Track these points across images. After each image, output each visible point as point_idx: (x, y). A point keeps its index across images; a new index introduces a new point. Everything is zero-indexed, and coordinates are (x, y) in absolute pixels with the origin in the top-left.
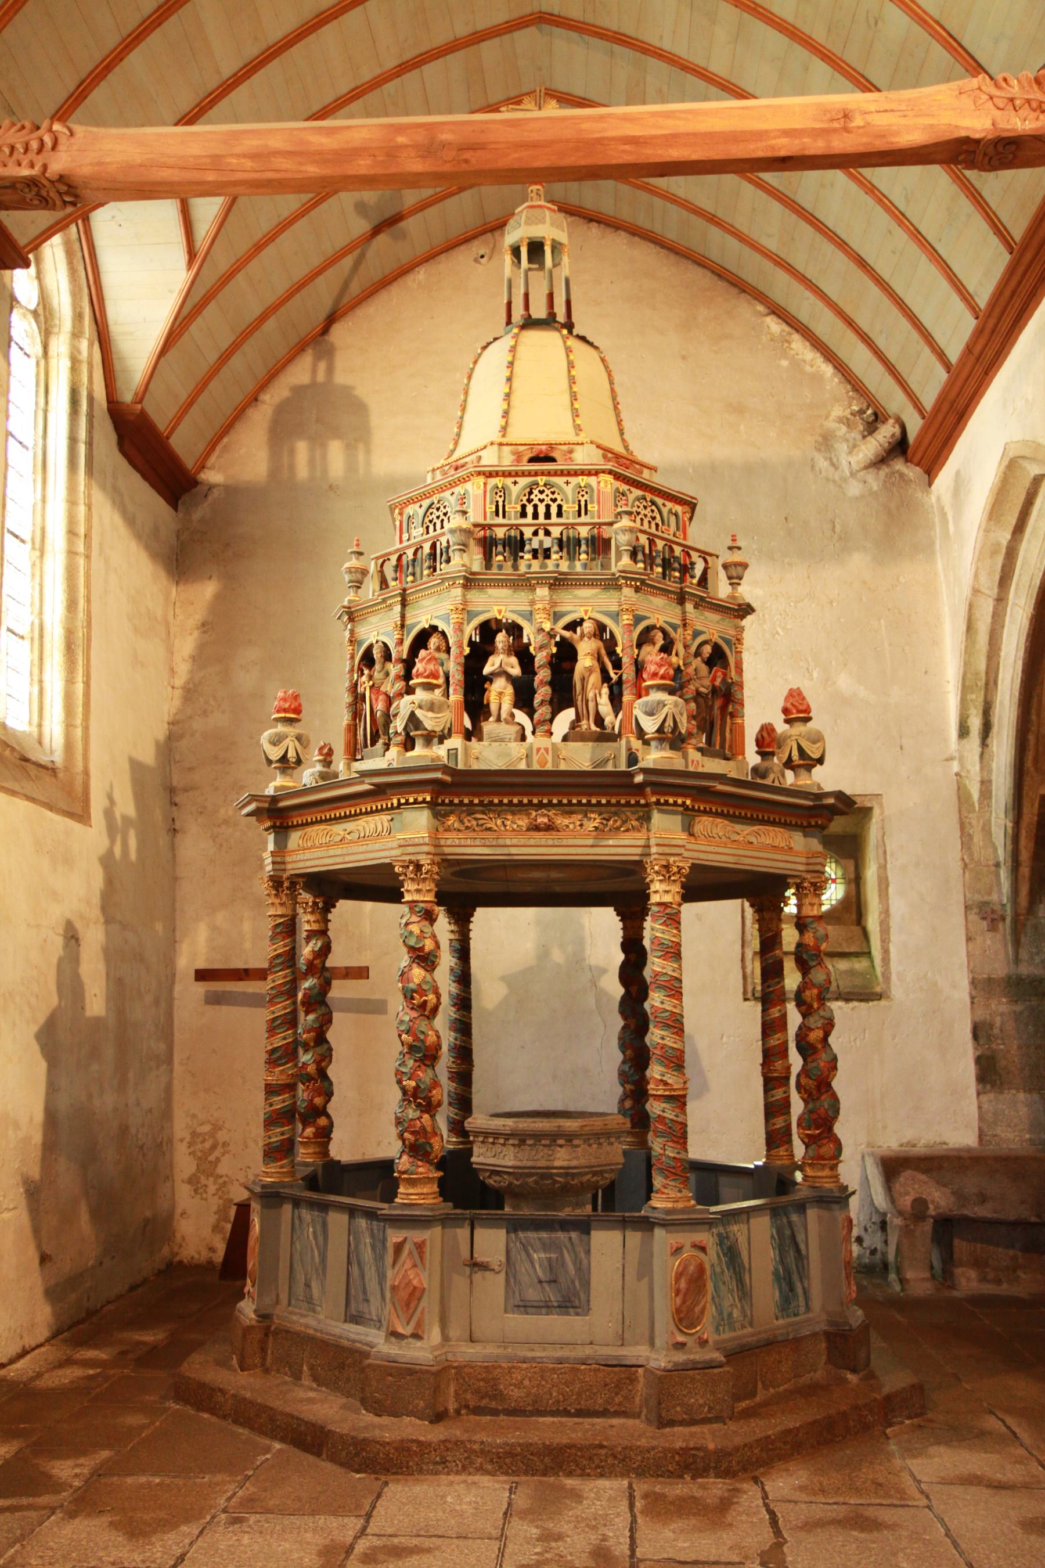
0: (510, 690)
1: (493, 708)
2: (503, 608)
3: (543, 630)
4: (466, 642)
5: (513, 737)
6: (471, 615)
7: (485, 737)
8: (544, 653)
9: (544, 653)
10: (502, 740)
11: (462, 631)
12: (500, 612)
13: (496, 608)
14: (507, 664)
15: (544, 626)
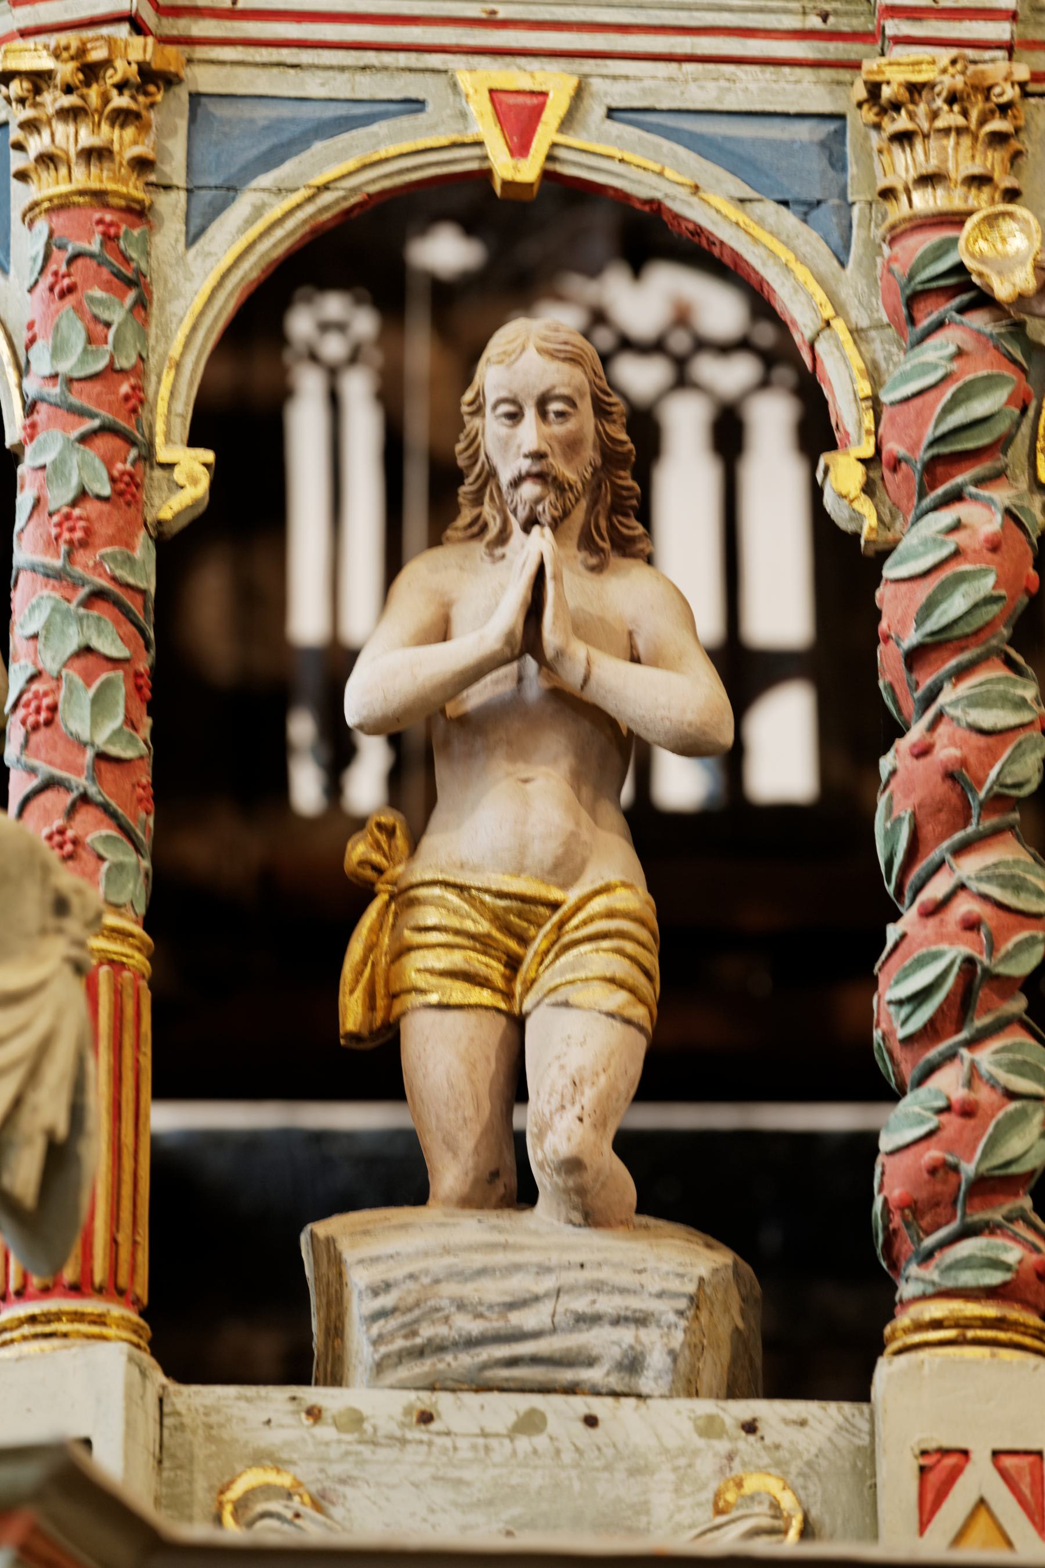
0: (614, 879)
1: (444, 1054)
2: (557, 82)
3: (966, 290)
4: (171, 402)
5: (658, 1346)
6: (233, 150)
7: (360, 1346)
8: (982, 518)
9: (982, 518)
10: (553, 1375)
11: (135, 285)
12: (519, 117)
13: (477, 79)
14: (582, 627)
15: (972, 248)
